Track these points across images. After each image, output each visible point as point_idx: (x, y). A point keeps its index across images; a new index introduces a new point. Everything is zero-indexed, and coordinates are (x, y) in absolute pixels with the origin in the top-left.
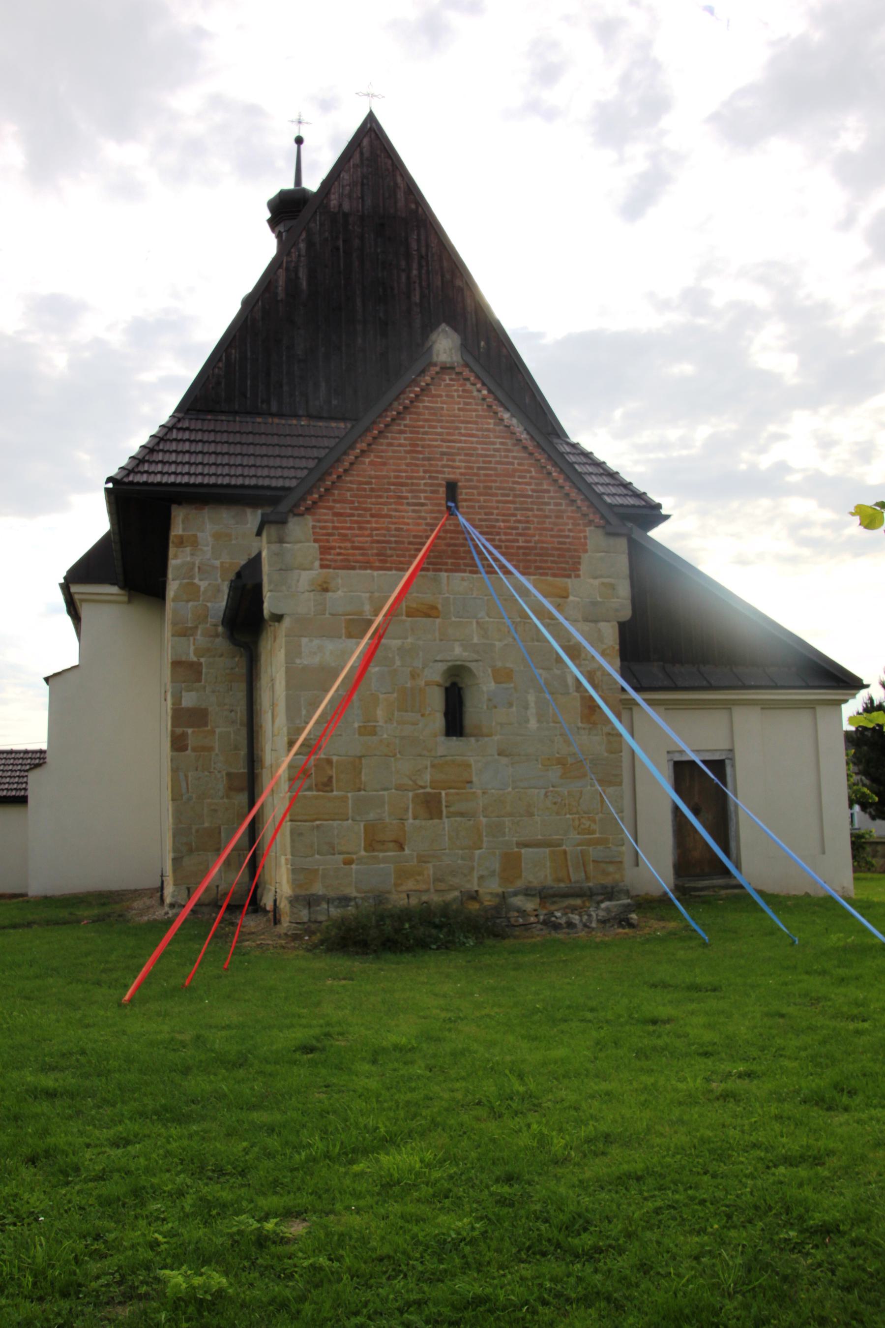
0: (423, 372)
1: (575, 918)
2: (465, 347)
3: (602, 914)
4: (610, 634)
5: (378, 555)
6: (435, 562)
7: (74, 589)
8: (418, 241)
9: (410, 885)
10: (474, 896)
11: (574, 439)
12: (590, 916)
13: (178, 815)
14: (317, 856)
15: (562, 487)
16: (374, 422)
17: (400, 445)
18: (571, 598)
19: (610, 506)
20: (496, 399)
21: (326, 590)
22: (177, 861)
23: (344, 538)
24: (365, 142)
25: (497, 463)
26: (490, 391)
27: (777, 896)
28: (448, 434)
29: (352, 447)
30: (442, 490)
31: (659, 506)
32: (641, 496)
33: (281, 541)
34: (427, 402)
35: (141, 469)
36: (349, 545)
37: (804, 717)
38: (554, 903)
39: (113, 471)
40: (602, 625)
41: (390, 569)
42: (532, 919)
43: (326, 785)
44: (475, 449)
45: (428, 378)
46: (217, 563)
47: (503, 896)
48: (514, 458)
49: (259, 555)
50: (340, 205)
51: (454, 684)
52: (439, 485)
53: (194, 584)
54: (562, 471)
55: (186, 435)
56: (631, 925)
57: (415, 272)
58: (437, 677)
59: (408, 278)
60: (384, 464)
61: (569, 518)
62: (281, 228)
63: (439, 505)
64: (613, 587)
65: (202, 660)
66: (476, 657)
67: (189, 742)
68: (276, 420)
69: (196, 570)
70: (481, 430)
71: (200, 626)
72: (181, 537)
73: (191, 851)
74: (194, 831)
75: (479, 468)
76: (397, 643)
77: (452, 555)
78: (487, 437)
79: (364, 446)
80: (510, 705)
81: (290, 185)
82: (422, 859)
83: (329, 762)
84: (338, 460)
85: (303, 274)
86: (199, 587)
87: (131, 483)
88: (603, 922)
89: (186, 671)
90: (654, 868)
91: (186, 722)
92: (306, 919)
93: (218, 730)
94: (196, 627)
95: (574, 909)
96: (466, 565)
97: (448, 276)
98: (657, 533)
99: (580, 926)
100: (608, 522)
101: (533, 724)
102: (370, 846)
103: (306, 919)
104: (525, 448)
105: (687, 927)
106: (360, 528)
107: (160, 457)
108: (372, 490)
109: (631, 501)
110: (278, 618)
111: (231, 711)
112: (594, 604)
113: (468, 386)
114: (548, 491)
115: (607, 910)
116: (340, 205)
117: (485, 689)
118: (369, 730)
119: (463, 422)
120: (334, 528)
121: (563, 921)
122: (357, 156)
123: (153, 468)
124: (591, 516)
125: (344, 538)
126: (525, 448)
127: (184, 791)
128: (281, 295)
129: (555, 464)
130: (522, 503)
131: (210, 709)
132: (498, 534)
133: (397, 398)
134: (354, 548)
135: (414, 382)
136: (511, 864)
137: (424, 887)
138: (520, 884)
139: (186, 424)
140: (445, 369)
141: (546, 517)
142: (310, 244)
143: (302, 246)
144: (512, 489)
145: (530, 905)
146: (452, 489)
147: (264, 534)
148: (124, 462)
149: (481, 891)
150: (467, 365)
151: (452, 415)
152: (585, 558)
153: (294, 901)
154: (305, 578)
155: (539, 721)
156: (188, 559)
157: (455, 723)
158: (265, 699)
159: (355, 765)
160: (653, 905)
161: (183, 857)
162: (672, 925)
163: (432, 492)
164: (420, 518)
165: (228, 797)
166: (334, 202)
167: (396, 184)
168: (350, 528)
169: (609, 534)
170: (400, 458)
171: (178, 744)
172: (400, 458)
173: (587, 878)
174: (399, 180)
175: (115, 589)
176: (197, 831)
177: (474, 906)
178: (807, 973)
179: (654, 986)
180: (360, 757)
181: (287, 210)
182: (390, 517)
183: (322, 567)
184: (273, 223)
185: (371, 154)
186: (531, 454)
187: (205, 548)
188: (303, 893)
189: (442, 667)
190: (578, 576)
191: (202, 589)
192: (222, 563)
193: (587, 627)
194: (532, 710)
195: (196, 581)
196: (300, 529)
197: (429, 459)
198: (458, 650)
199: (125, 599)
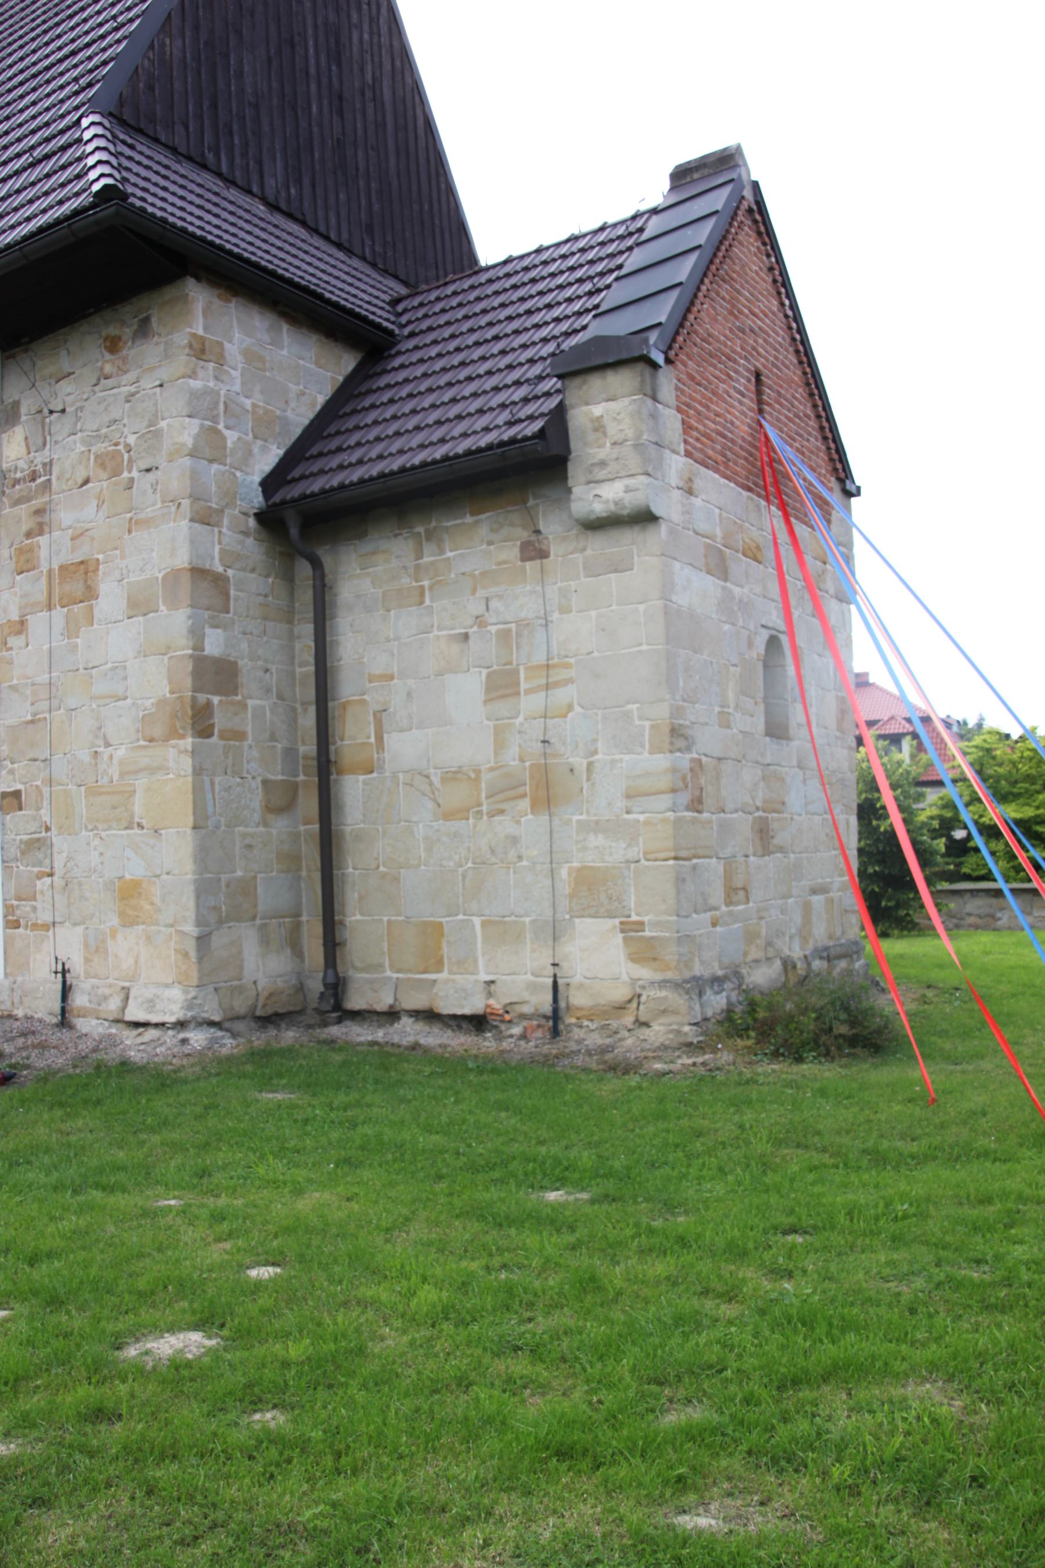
13: (202, 856)
14: (694, 915)
46: (248, 403)
53: (218, 432)
65: (230, 573)
67: (216, 720)
69: (222, 407)
71: (227, 511)
73: (220, 922)
74: (223, 885)
86: (224, 439)
93: (250, 703)
94: (222, 511)
111: (267, 671)
131: (241, 663)
156: (211, 384)
161: (210, 933)
165: (266, 824)
176: (228, 886)
180: (719, 759)
187: (232, 372)
191: (229, 444)
192: (254, 405)
195: (221, 427)
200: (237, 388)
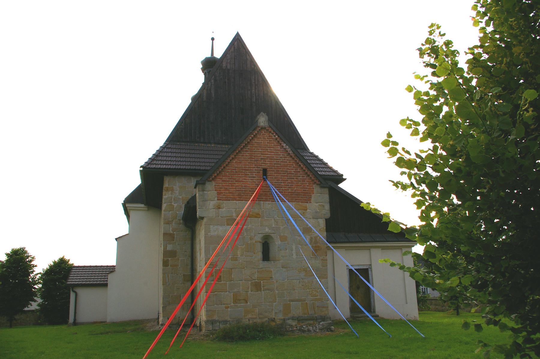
0: (254, 129)
1: (311, 328)
2: (270, 120)
3: (320, 326)
4: (322, 223)
6: (258, 198)
8: (255, 79)
9: (250, 316)
10: (273, 320)
11: (311, 151)
12: (316, 327)
13: (165, 290)
15: (305, 170)
16: (237, 148)
17: (246, 156)
18: (308, 210)
20: (281, 139)
21: (219, 208)
23: (226, 189)
24: (236, 43)
26: (278, 136)
27: (388, 320)
29: (229, 156)
30: (261, 172)
31: (342, 175)
32: (336, 172)
33: (203, 191)
34: (256, 140)
35: (153, 163)
36: (228, 192)
38: (303, 322)
39: (143, 163)
40: (319, 220)
42: (295, 329)
43: (219, 279)
44: (273, 157)
45: (256, 132)
46: (181, 197)
47: (284, 320)
48: (288, 160)
49: (196, 195)
50: (226, 66)
51: (266, 242)
52: (260, 170)
53: (172, 205)
54: (304, 165)
55: (170, 150)
56: (332, 331)
58: (260, 240)
59: (251, 93)
60: (240, 163)
62: (206, 71)
64: (323, 206)
66: (274, 232)
68: (203, 145)
70: (276, 150)
72: (167, 188)
77: (265, 195)
78: (278, 153)
79: (233, 156)
84: (224, 161)
85: (213, 91)
87: (149, 168)
88: (321, 329)
89: (168, 237)
90: (341, 309)
91: (168, 257)
92: (211, 329)
95: (310, 325)
96: (270, 199)
98: (341, 185)
99: (312, 331)
100: (321, 183)
101: (294, 256)
103: (211, 329)
104: (291, 156)
105: (352, 332)
106: (232, 186)
107: (160, 158)
108: (236, 172)
109: (332, 174)
110: (202, 218)
112: (316, 212)
113: (271, 134)
115: (323, 325)
116: (226, 66)
118: (235, 259)
121: (306, 329)
122: (233, 49)
123: (157, 162)
124: (315, 181)
126: (291, 156)
129: (302, 162)
130: (290, 176)
132: (282, 187)
135: (251, 133)
137: (254, 317)
139: (170, 146)
140: (263, 128)
143: (213, 81)
144: (286, 171)
145: (294, 323)
146: (265, 171)
149: (276, 318)
150: (270, 127)
151: (265, 146)
152: (313, 196)
153: (207, 322)
154: (212, 204)
155: (297, 255)
157: (266, 256)
158: (198, 248)
160: (339, 323)
162: (346, 331)
166: (224, 65)
167: (247, 59)
168: (228, 186)
169: (322, 187)
171: (165, 264)
172: (246, 161)
174: (248, 57)
175: (143, 205)
177: (273, 324)
178: (391, 347)
179: (335, 352)
180: (231, 269)
182: (243, 182)
183: (218, 200)
184: (203, 70)
185: (238, 46)
186: (293, 159)
189: (261, 236)
190: (310, 202)
193: (313, 221)
194: (294, 251)
196: (210, 186)
197: (257, 161)
198: (267, 230)
199: (146, 209)
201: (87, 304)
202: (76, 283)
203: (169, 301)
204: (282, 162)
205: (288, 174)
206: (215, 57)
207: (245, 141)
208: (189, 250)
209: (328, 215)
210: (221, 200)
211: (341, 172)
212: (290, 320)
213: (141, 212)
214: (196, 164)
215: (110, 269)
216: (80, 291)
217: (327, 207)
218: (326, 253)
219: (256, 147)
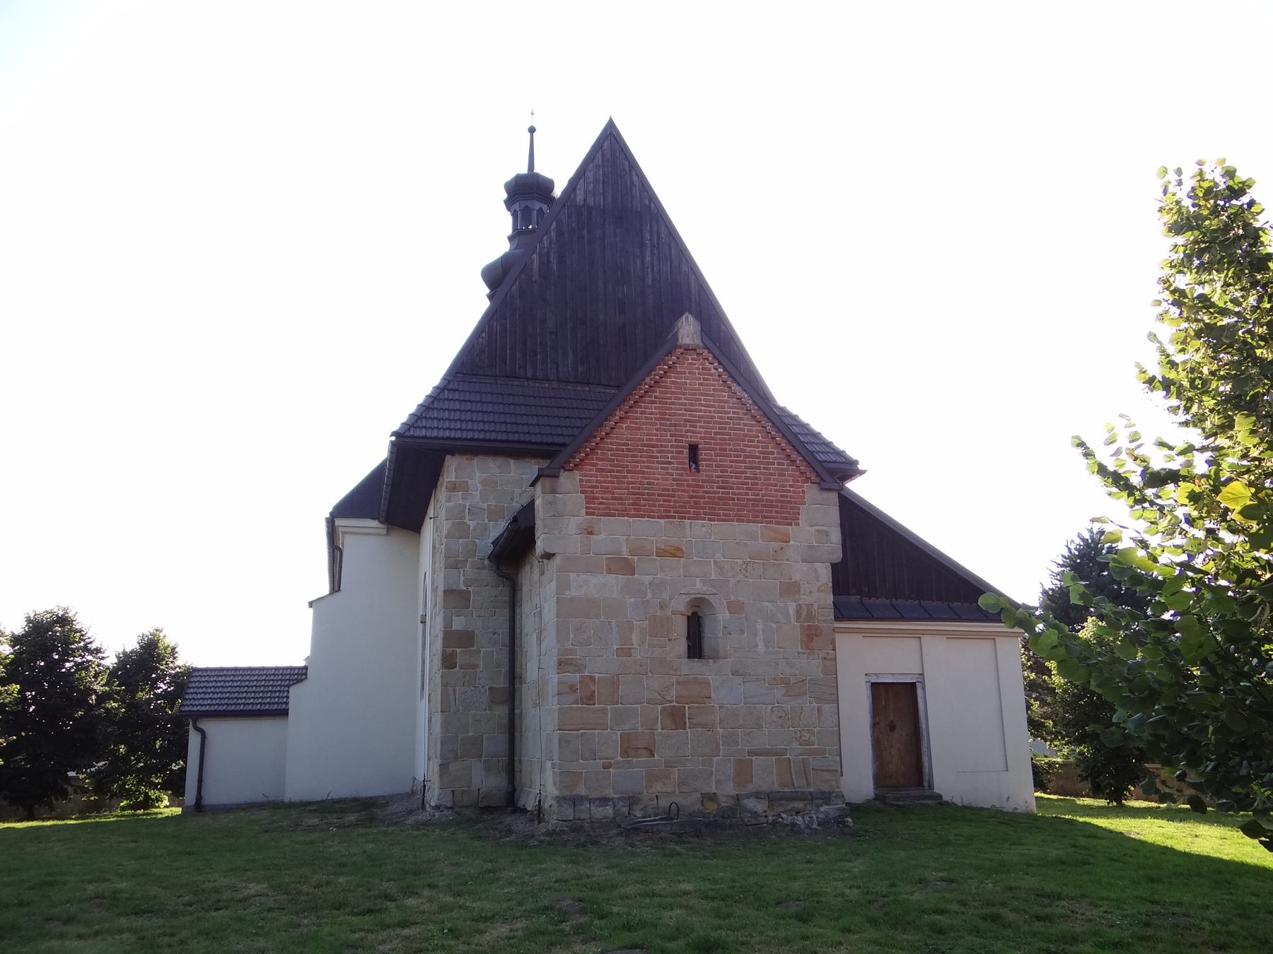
0: (670, 353)
1: (799, 820)
3: (821, 816)
4: (824, 574)
5: (633, 504)
7: (338, 522)
9: (659, 787)
10: (713, 798)
13: (446, 725)
19: (820, 462)
20: (731, 376)
21: (591, 533)
22: (443, 767)
23: (606, 490)
24: (606, 144)
25: (731, 429)
26: (725, 369)
28: (691, 405)
29: (612, 414)
31: (856, 463)
32: (840, 454)
33: (554, 492)
34: (673, 378)
35: (419, 424)
37: (986, 646)
39: (396, 427)
41: (643, 516)
42: (764, 820)
43: (590, 699)
44: (712, 417)
46: (485, 506)
47: (738, 798)
48: (746, 425)
49: (532, 503)
51: (695, 613)
52: (683, 447)
55: (456, 396)
57: (648, 259)
58: (682, 608)
60: (639, 429)
61: (790, 475)
62: (516, 207)
63: (683, 463)
65: (470, 589)
68: (531, 384)
72: (454, 483)
73: (456, 757)
75: (716, 433)
76: (647, 579)
80: (742, 632)
81: (524, 170)
82: (669, 764)
83: (592, 679)
84: (601, 425)
85: (553, 259)
87: (413, 437)
89: (455, 598)
90: (858, 779)
91: (456, 645)
97: (676, 263)
98: (854, 486)
101: (761, 648)
102: (626, 752)
108: (628, 450)
110: (549, 556)
114: (772, 453)
117: (720, 617)
118: (625, 652)
119: (703, 395)
120: (597, 481)
122: (599, 156)
123: (429, 424)
125: (606, 490)
126: (754, 417)
127: (452, 703)
128: (536, 277)
133: (649, 374)
134: (614, 499)
136: (743, 770)
137: (669, 789)
138: (751, 788)
139: (456, 387)
140: (688, 349)
141: (771, 474)
142: (560, 233)
143: (553, 234)
146: (693, 449)
147: (539, 485)
148: (404, 418)
150: (706, 348)
153: (560, 800)
154: (573, 524)
157: (696, 649)
158: (528, 622)
159: (614, 682)
163: (678, 452)
164: (668, 474)
166: (580, 197)
167: (632, 182)
170: (651, 424)
171: (448, 661)
172: (651, 424)
173: (808, 784)
174: (635, 178)
175: (375, 523)
177: (711, 807)
181: (526, 193)
184: (509, 203)
188: (568, 793)
189: (687, 599)
190: (797, 524)
194: (760, 639)
196: (569, 481)
198: (699, 585)
199: (384, 531)
200: (478, 499)
201: (231, 759)
202: (204, 708)
203: (453, 750)
204: (731, 429)
205: (746, 457)
206: (537, 175)
207: (648, 380)
208: (504, 630)
209: (838, 556)
210: (593, 514)
211: (852, 453)
212: (752, 800)
213: (368, 540)
214: (543, 430)
215: (296, 675)
216: (210, 726)
217: (836, 536)
218: (833, 642)
219: (672, 393)
